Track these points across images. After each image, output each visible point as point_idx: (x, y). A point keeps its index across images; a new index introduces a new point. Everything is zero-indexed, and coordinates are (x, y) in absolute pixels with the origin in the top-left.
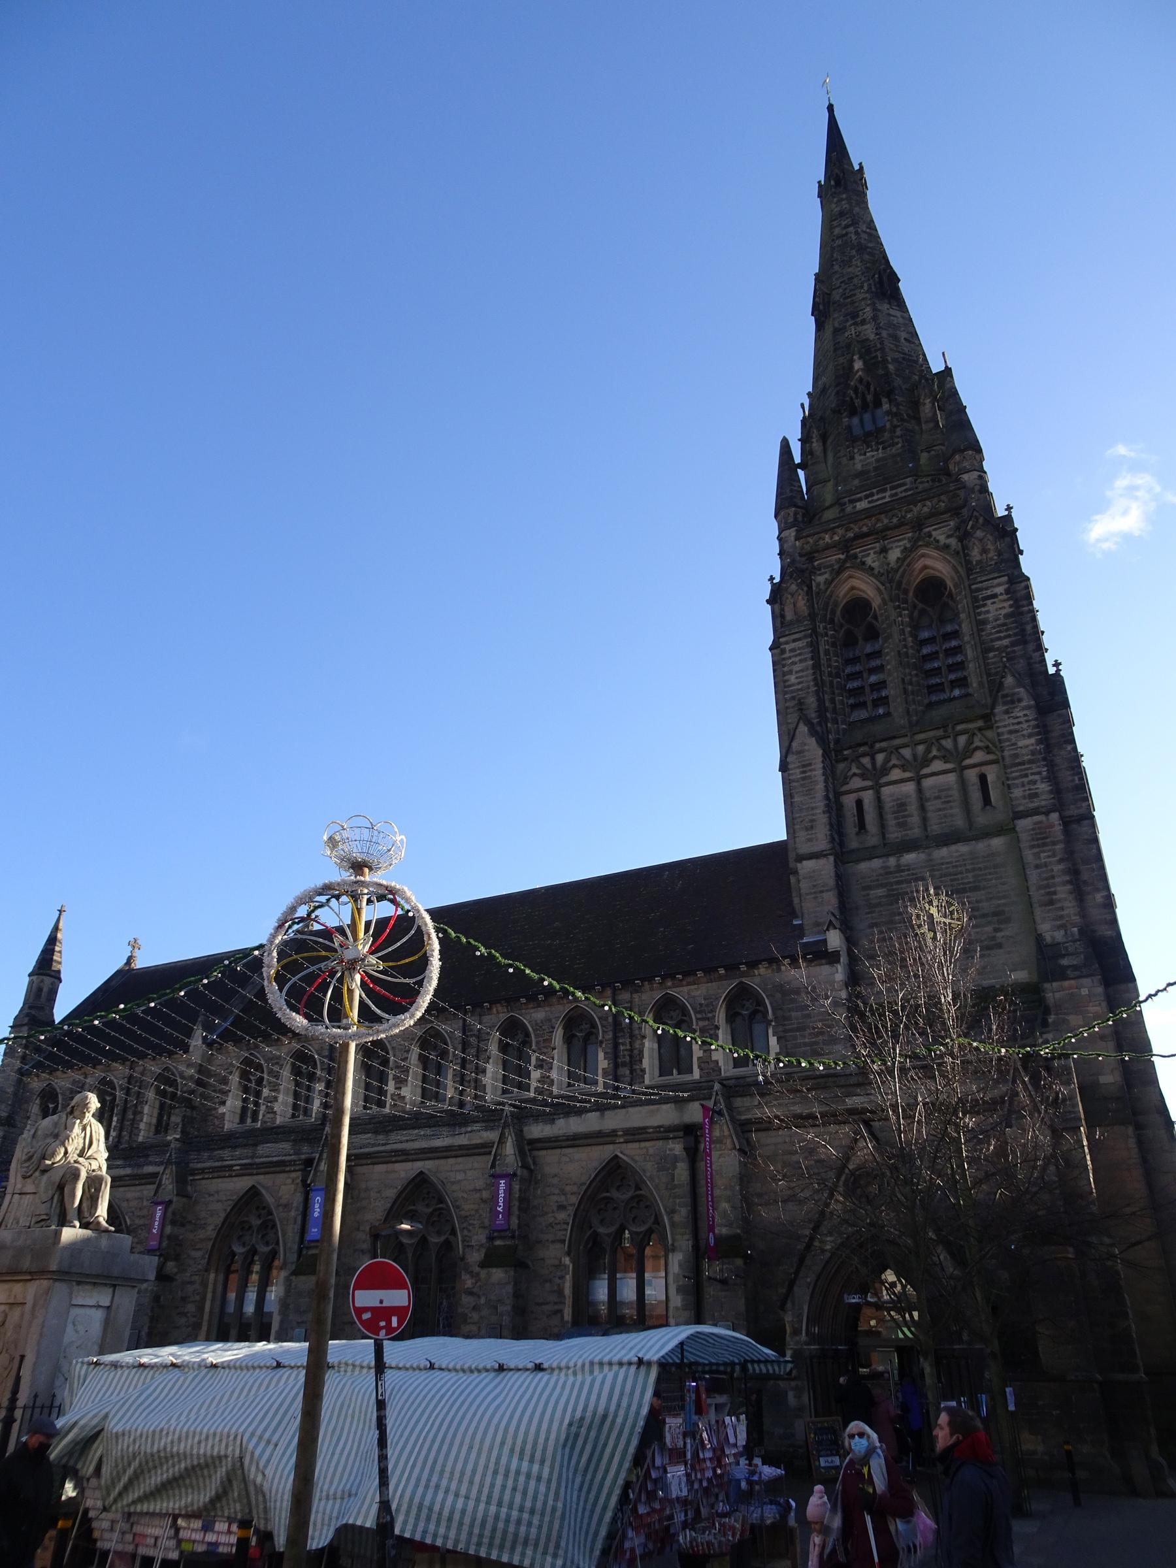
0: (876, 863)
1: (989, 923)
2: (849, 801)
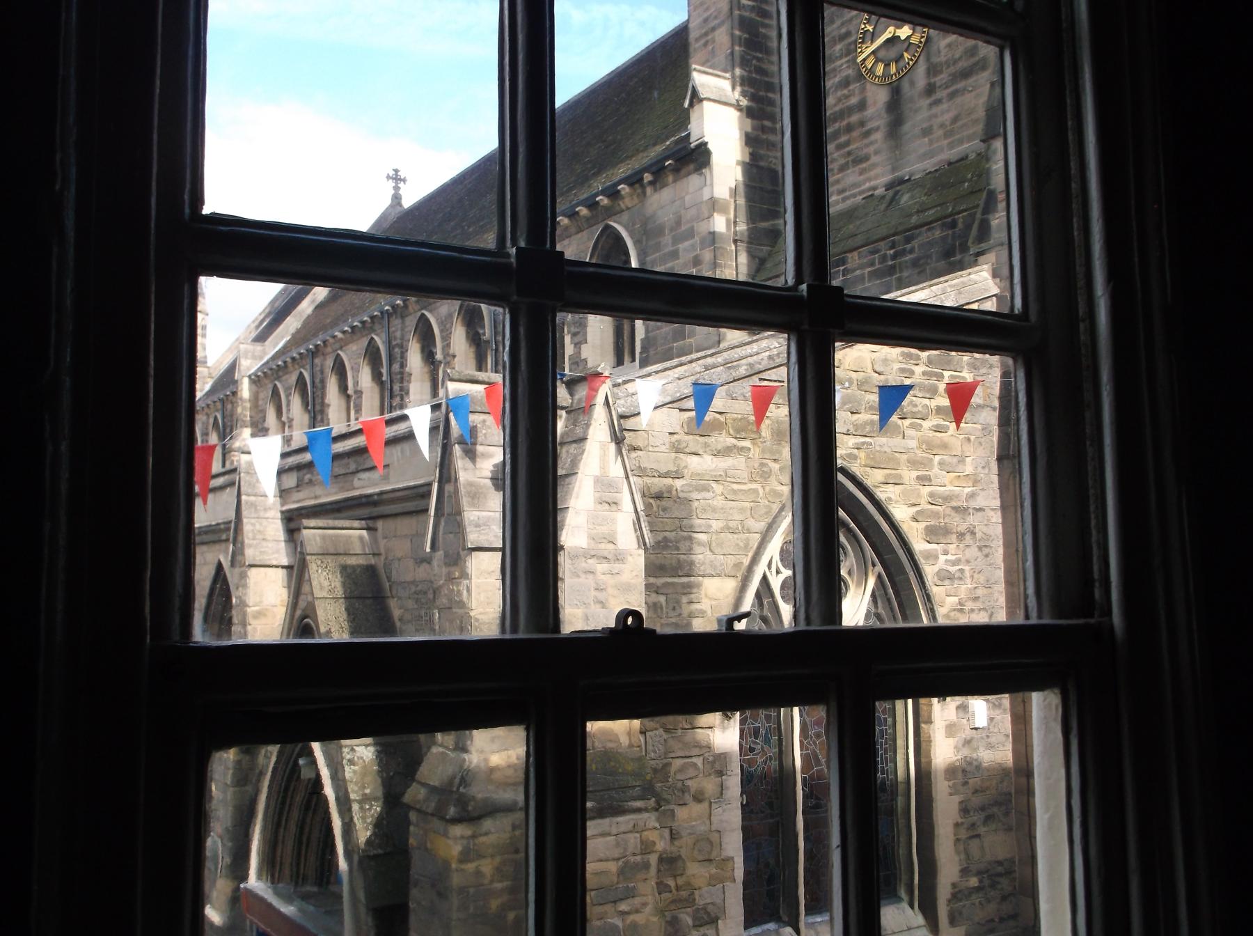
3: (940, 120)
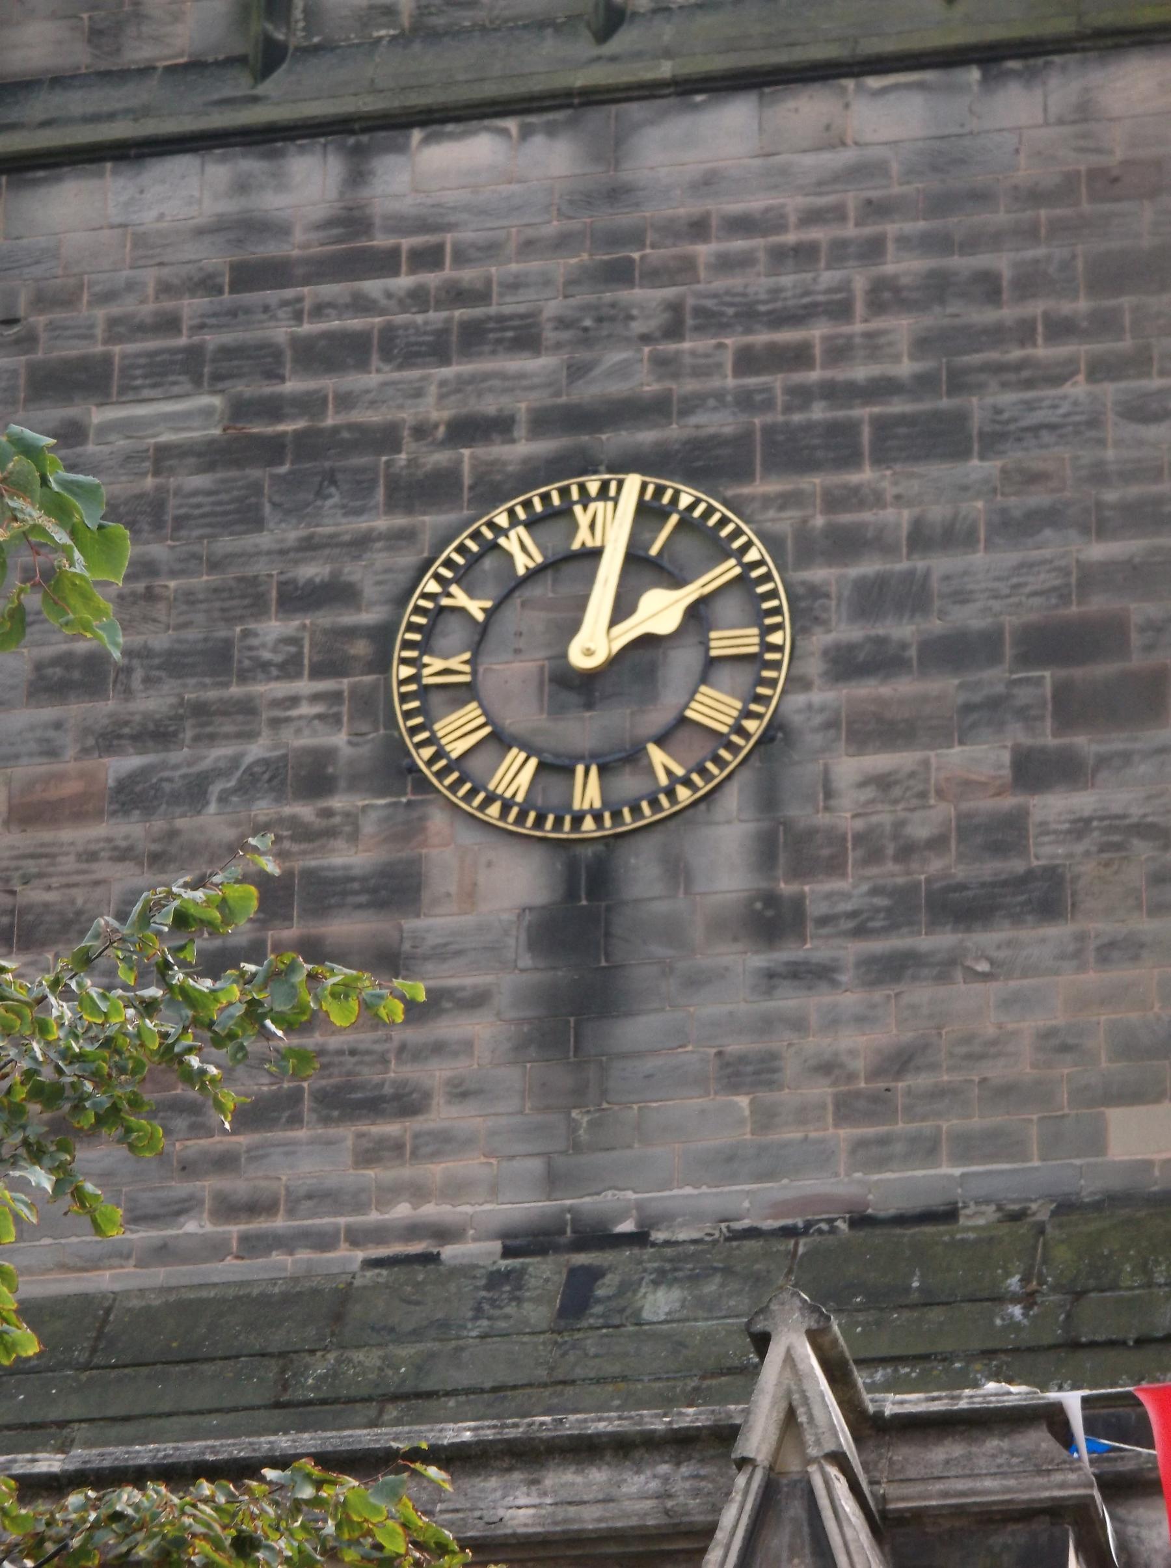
0: (182, 197)
3: (817, 1044)
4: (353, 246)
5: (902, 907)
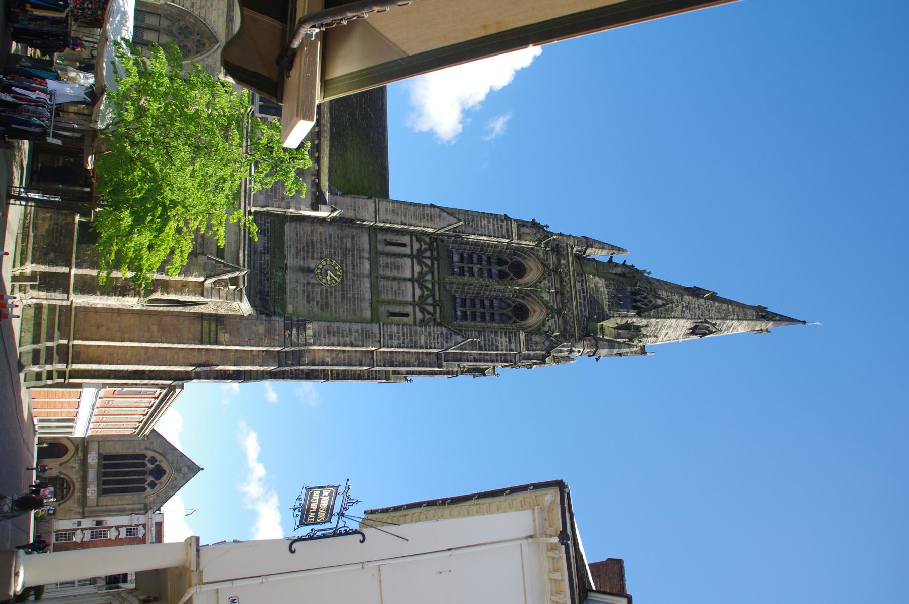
1: (322, 299)
2: (406, 239)
4: (361, 258)
5: (308, 292)
